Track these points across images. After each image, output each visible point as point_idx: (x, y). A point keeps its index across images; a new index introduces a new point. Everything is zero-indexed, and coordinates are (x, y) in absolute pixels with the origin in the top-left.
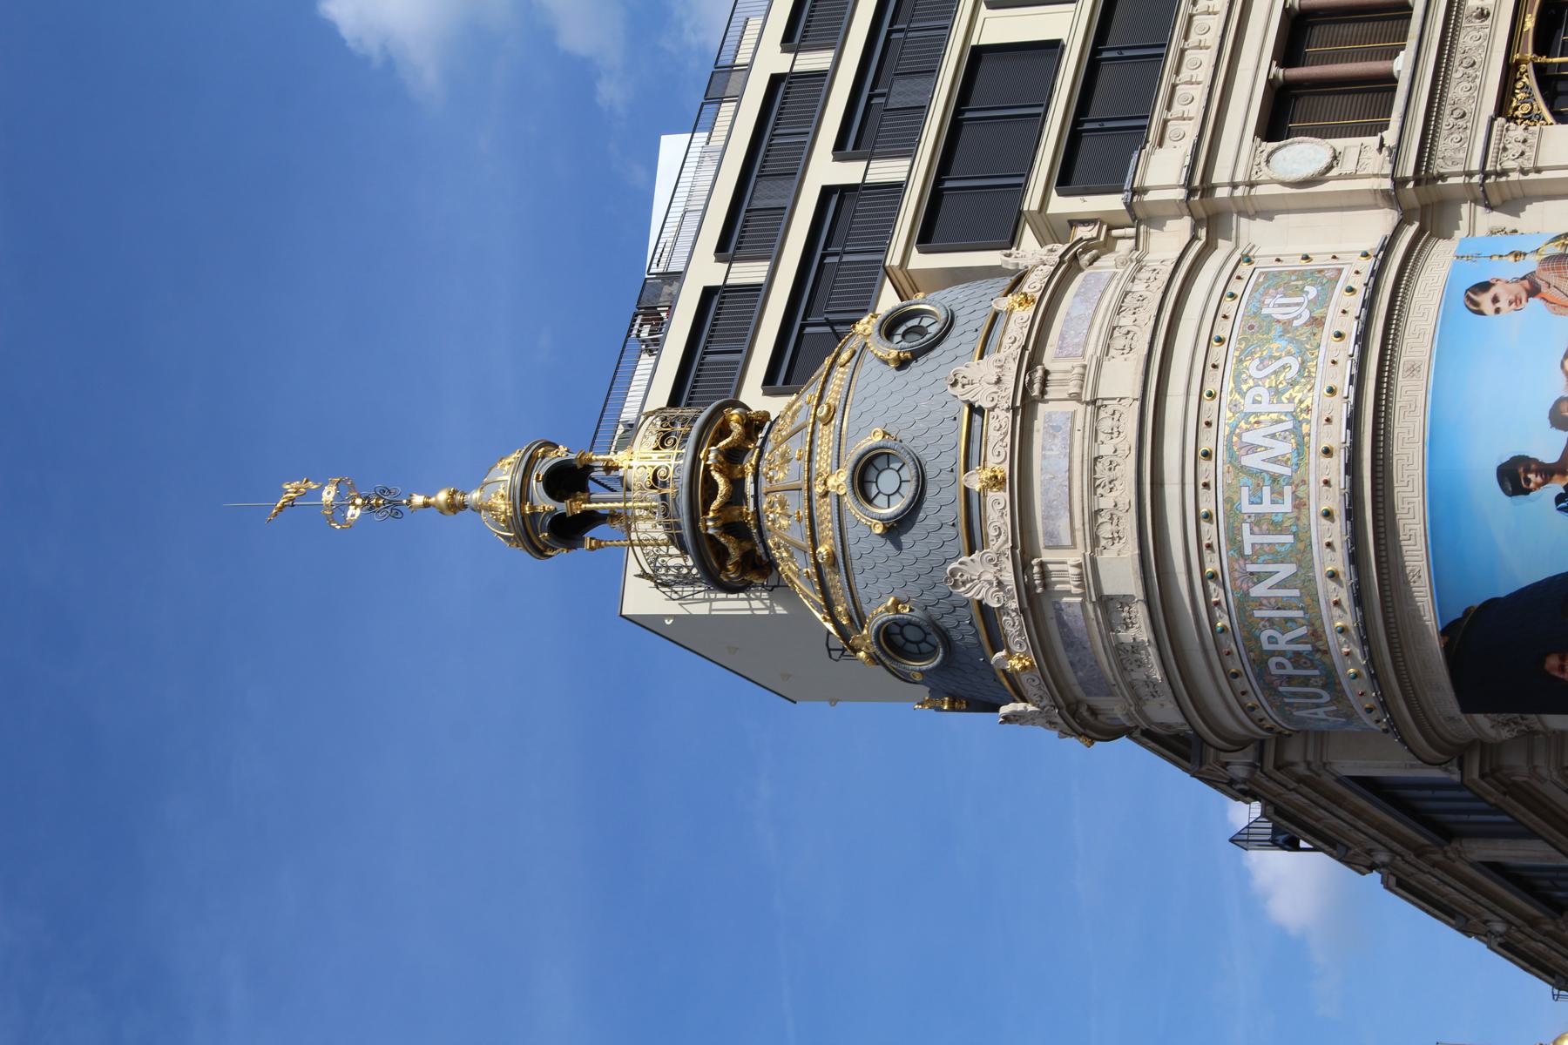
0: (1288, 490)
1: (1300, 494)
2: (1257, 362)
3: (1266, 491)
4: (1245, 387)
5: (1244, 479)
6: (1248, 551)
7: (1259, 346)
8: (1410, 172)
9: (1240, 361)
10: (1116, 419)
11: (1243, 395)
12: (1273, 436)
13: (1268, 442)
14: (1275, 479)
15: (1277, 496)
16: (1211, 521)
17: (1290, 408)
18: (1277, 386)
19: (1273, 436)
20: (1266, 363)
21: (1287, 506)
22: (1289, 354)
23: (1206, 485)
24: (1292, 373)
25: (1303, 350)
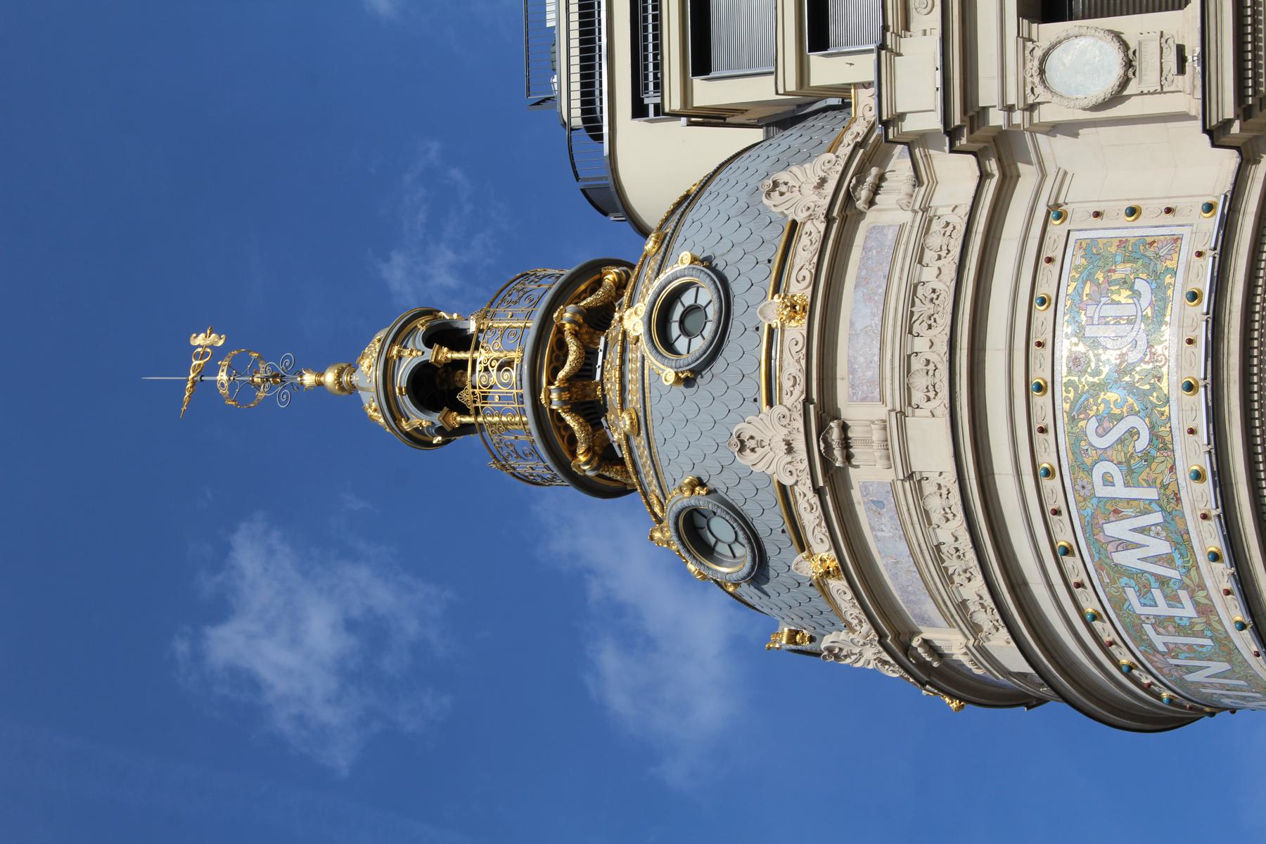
0: (1183, 595)
1: (1204, 601)
2: (1093, 423)
3: (1157, 593)
4: (1088, 461)
5: (1124, 580)
6: (1162, 648)
7: (1092, 396)
8: (1229, 111)
9: (1073, 420)
10: (948, 233)
11: (1089, 471)
12: (1143, 530)
13: (1138, 538)
14: (1163, 582)
15: (1173, 600)
16: (1102, 620)
17: (1152, 494)
18: (1128, 462)
19: (1143, 530)
20: (1106, 424)
21: (1188, 611)
22: (1132, 413)
23: (1079, 585)
24: (1142, 443)
25: (1149, 406)
